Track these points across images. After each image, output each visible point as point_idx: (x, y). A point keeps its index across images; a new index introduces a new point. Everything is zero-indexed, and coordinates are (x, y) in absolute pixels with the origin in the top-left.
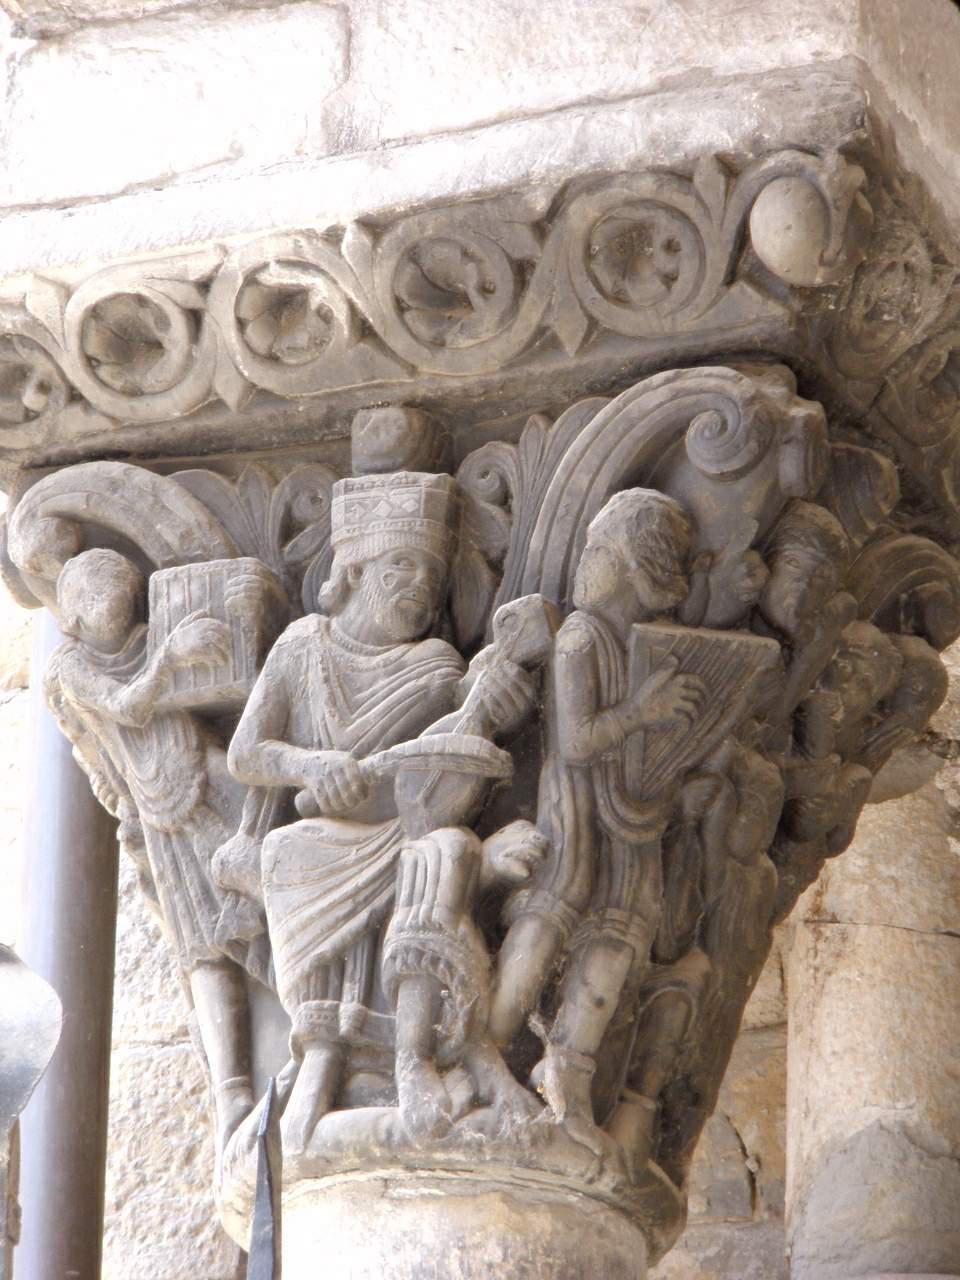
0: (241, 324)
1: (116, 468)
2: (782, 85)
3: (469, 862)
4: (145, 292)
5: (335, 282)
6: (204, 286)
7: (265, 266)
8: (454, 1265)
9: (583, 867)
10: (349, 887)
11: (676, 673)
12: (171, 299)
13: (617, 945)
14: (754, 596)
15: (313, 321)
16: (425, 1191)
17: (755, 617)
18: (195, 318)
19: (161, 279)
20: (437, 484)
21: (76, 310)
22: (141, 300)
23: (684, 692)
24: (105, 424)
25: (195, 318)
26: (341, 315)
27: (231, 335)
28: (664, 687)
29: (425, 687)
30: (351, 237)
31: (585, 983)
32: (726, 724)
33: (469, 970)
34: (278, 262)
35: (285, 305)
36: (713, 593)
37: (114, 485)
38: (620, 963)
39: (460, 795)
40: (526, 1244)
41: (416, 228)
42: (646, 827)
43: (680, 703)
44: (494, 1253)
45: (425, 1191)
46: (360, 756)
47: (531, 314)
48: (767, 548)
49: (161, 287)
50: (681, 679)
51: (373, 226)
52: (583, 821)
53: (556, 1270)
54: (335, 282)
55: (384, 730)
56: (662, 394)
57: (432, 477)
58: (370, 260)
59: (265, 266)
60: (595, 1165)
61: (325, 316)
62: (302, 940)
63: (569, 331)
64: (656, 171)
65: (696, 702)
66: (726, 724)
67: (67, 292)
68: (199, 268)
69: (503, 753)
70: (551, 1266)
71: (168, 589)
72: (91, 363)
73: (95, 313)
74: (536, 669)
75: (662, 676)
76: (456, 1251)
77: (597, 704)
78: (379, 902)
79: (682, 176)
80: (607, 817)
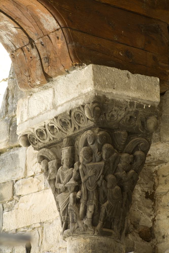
0: (50, 130)
1: (44, 149)
2: (86, 95)
3: (74, 197)
6: (45, 127)
7: (49, 124)
8: (78, 248)
9: (86, 196)
10: (65, 201)
11: (92, 169)
12: (42, 129)
13: (92, 204)
14: (100, 157)
15: (55, 129)
16: (75, 239)
17: (101, 159)
18: (45, 130)
20: (70, 148)
23: (93, 172)
24: (43, 144)
27: (49, 132)
28: (90, 172)
29: (70, 175)
31: (89, 210)
32: (100, 174)
33: (75, 211)
35: (52, 127)
36: (96, 158)
37: (45, 151)
38: (93, 206)
39: (73, 189)
40: (86, 244)
42: (93, 189)
43: (93, 173)
44: (82, 245)
45: (75, 239)
46: (65, 185)
48: (100, 150)
50: (92, 170)
51: (56, 118)
52: (85, 190)
53: (90, 246)
55: (66, 181)
56: (85, 135)
57: (69, 147)
60: (93, 232)
63: (77, 127)
64: (77, 108)
65: (95, 173)
66: (100, 174)
67: (34, 129)
68: (43, 125)
69: (76, 183)
70: (90, 246)
71: (50, 164)
72: (39, 137)
73: (37, 131)
74: (78, 171)
75: (90, 170)
76: (78, 246)
77: (84, 175)
78: (68, 202)
79: (79, 108)
80: (88, 189)
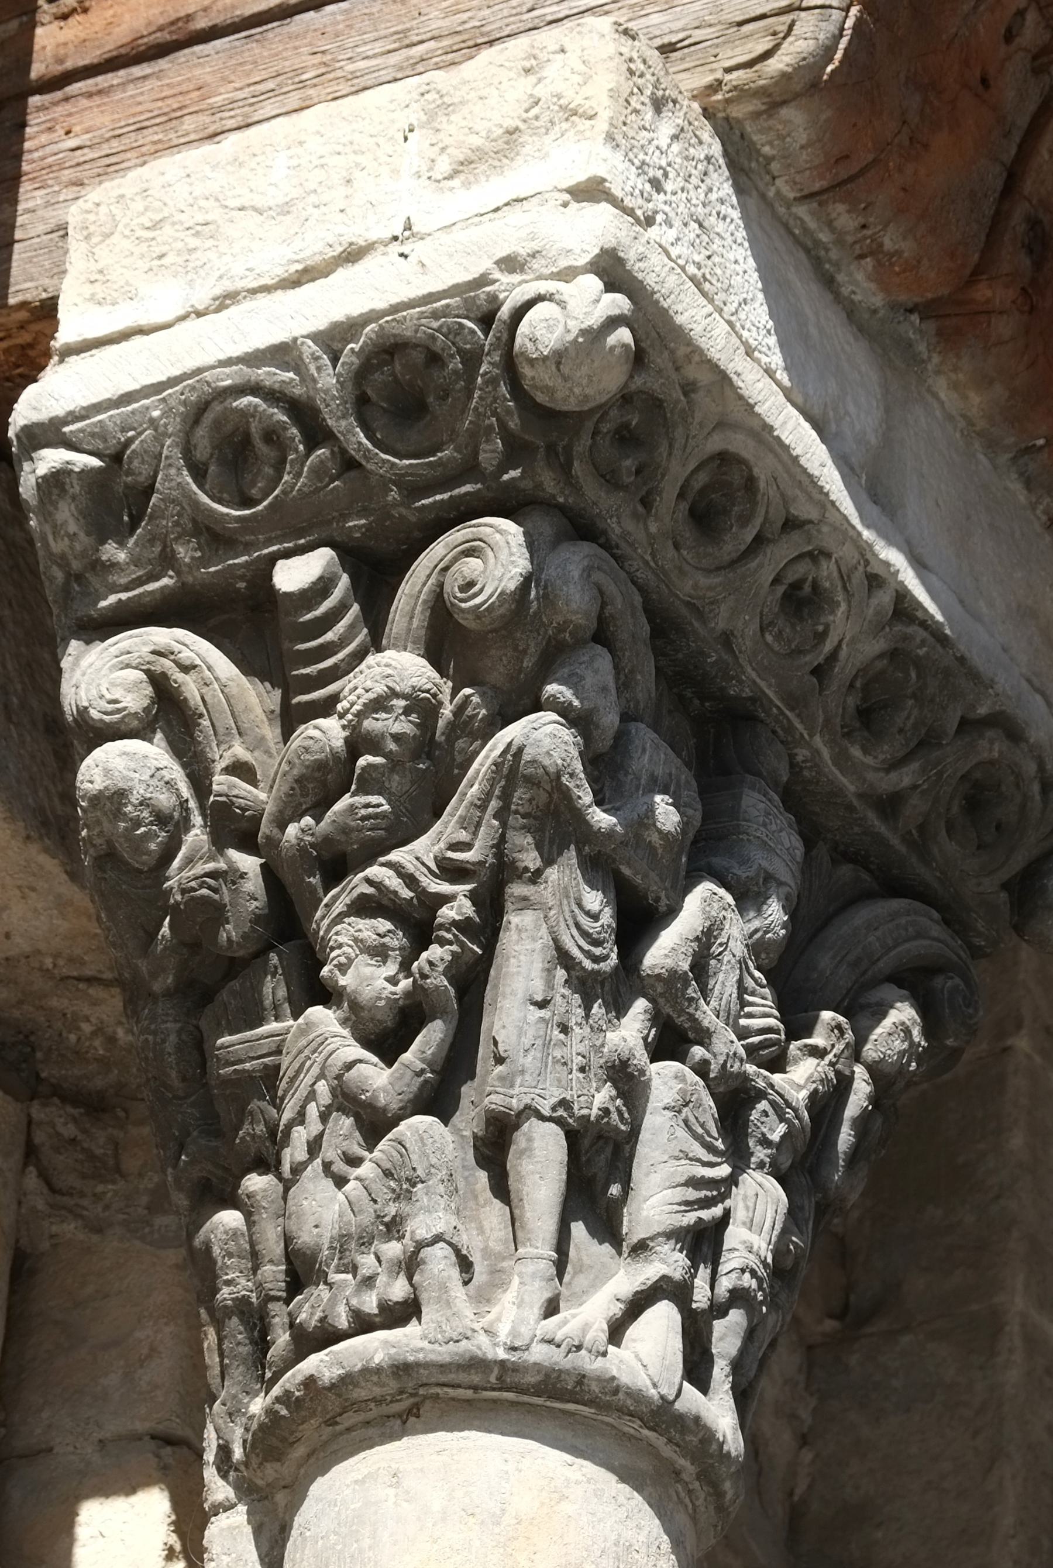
4: (762, 485)
5: (848, 618)
6: (791, 524)
19: (778, 486)
21: (716, 443)
22: (750, 484)
25: (759, 540)
26: (828, 646)
30: (884, 599)
34: (836, 561)
41: (918, 640)
47: (905, 778)
49: (772, 492)
54: (848, 618)
58: (878, 628)
59: (828, 556)
61: (821, 637)
62: (692, 1194)
68: (804, 510)
73: (724, 459)
